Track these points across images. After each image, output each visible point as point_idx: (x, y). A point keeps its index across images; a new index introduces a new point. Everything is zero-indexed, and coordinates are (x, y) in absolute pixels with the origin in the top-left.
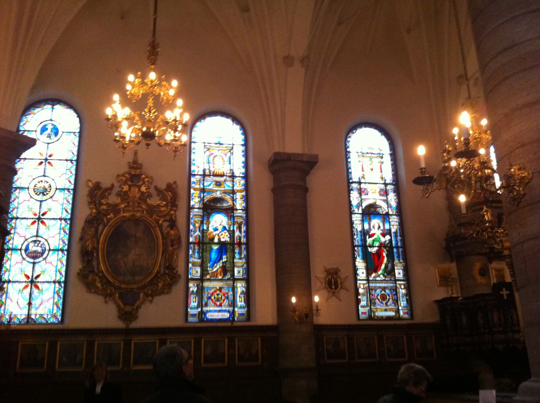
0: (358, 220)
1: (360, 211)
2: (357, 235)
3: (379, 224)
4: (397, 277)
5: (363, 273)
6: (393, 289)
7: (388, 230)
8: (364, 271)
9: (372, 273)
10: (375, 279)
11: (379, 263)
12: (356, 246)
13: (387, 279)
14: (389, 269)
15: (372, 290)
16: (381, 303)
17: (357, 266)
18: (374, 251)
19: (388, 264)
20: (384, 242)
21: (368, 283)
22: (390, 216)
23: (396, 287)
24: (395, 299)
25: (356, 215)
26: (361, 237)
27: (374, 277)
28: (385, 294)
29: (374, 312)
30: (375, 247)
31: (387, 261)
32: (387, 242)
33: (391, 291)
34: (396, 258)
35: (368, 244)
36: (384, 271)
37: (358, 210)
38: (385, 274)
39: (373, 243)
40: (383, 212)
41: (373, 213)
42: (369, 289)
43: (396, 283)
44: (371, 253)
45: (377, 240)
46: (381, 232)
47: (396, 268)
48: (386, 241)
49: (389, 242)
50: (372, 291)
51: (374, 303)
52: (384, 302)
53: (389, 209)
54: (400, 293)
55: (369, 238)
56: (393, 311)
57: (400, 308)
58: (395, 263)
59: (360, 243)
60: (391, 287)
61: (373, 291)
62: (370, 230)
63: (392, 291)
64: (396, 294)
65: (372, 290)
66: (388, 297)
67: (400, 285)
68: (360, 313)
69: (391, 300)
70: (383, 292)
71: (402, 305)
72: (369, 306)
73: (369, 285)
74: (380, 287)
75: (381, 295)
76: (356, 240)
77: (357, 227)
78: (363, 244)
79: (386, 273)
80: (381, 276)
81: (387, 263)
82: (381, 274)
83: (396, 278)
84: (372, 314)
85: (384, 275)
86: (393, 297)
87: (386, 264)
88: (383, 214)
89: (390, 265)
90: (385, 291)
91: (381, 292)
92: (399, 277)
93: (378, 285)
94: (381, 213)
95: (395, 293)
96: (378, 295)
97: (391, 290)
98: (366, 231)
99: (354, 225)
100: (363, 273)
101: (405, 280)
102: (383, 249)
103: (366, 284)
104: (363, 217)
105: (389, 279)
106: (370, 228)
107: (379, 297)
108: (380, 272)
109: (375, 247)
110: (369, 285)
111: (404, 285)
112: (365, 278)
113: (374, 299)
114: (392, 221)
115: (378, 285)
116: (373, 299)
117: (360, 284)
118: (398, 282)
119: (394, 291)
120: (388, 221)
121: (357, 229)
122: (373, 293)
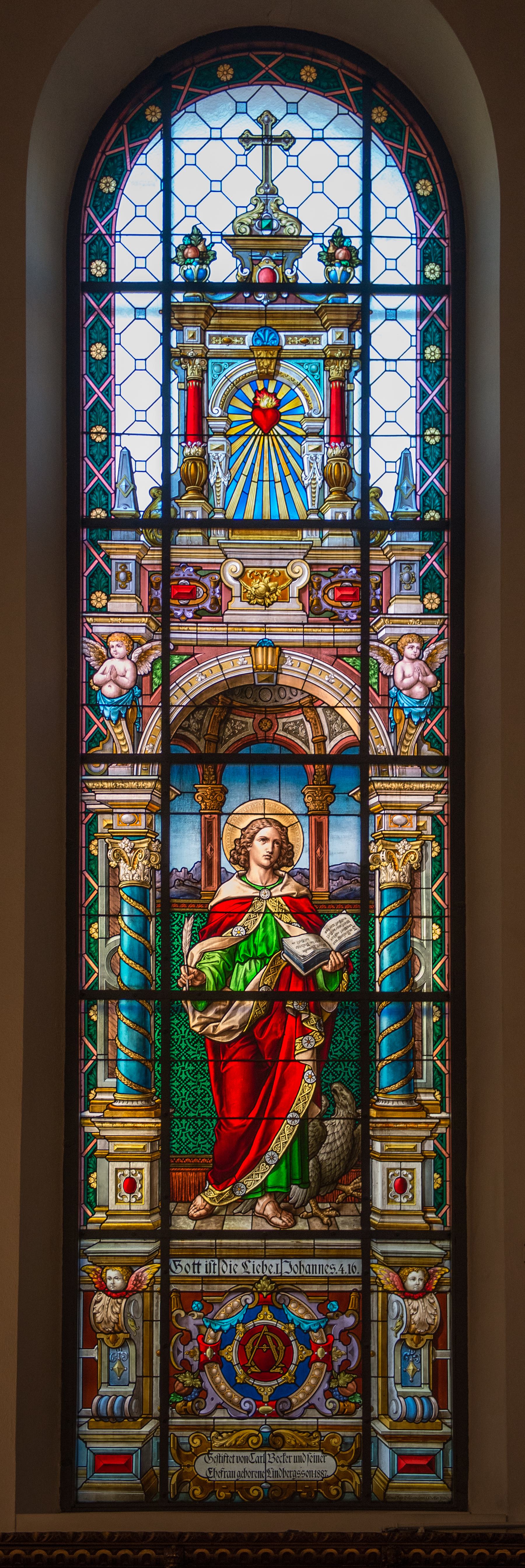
0: (131, 805)
1: (150, 744)
2: (113, 916)
3: (283, 830)
4: (383, 1214)
5: (131, 1186)
6: (343, 1298)
7: (346, 871)
8: (143, 1171)
9: (200, 1190)
10: (212, 1225)
11: (253, 1114)
12: (94, 995)
13: (302, 1225)
14: (323, 1155)
15: (186, 1300)
16: (244, 1390)
17: (90, 1137)
18: (229, 1031)
19: (321, 1118)
20: (306, 967)
21: (165, 1255)
22: (372, 771)
23: (366, 1277)
24: (347, 1362)
25: (117, 770)
26: (144, 933)
27: (211, 1213)
28: (280, 1326)
29: (187, 1456)
30: (243, 996)
31: (316, 1100)
32: (335, 959)
33: (322, 1308)
34: (385, 1077)
35: (183, 979)
36: (289, 1167)
37: (136, 737)
38: (297, 1192)
39: (227, 974)
40: (321, 741)
41: (245, 751)
42: (165, 1294)
43: (366, 1256)
44: (204, 1038)
45: (262, 950)
46: (291, 888)
47: (377, 1146)
48: (322, 956)
49: (347, 964)
50: (188, 1311)
51: (187, 1392)
52: (266, 1389)
53: (375, 716)
54: (391, 1325)
55: (201, 935)
56: (324, 1448)
57: (381, 1427)
58: (373, 1113)
59: (129, 976)
60: (329, 1280)
61: (196, 1305)
62: (209, 882)
63: (334, 1306)
64: (362, 1330)
65: (186, 1300)
66: (298, 1353)
67: (399, 1266)
68: (85, 1459)
69: (317, 1371)
70: (265, 1317)
71: (397, 1407)
72: (156, 1411)
73: (165, 1269)
74: (245, 1284)
75: (248, 1334)
76: (103, 952)
77: (119, 856)
78: (146, 981)
79: (304, 1183)
80: (266, 1206)
81: (317, 1110)
82: (263, 1188)
83: (375, 1219)
84: (173, 1466)
85: (281, 1199)
86: (339, 1348)
87: (304, 1121)
88: (320, 759)
89: (336, 1128)
90: (280, 1313)
91: (251, 1314)
92: (395, 1207)
93: (237, 1267)
94: (312, 750)
95: (349, 1321)
96: (227, 1336)
97: (322, 1300)
98: (182, 883)
99: (97, 848)
100: (131, 1186)
101: (436, 1227)
102: (298, 1014)
103: (148, 1259)
104: (165, 780)
105: (317, 1225)
106: (208, 861)
107: (231, 1353)
108: (252, 1182)
109: (243, 996)
110: (165, 1269)
111: (427, 1266)
112: (144, 1223)
113: (196, 1365)
114: (384, 805)
115: (237, 1267)
116: (186, 1365)
117: (103, 1262)
118: (380, 1248)
119: (343, 1310)
120: (356, 808)
121: (113, 872)
122: (192, 1323)
